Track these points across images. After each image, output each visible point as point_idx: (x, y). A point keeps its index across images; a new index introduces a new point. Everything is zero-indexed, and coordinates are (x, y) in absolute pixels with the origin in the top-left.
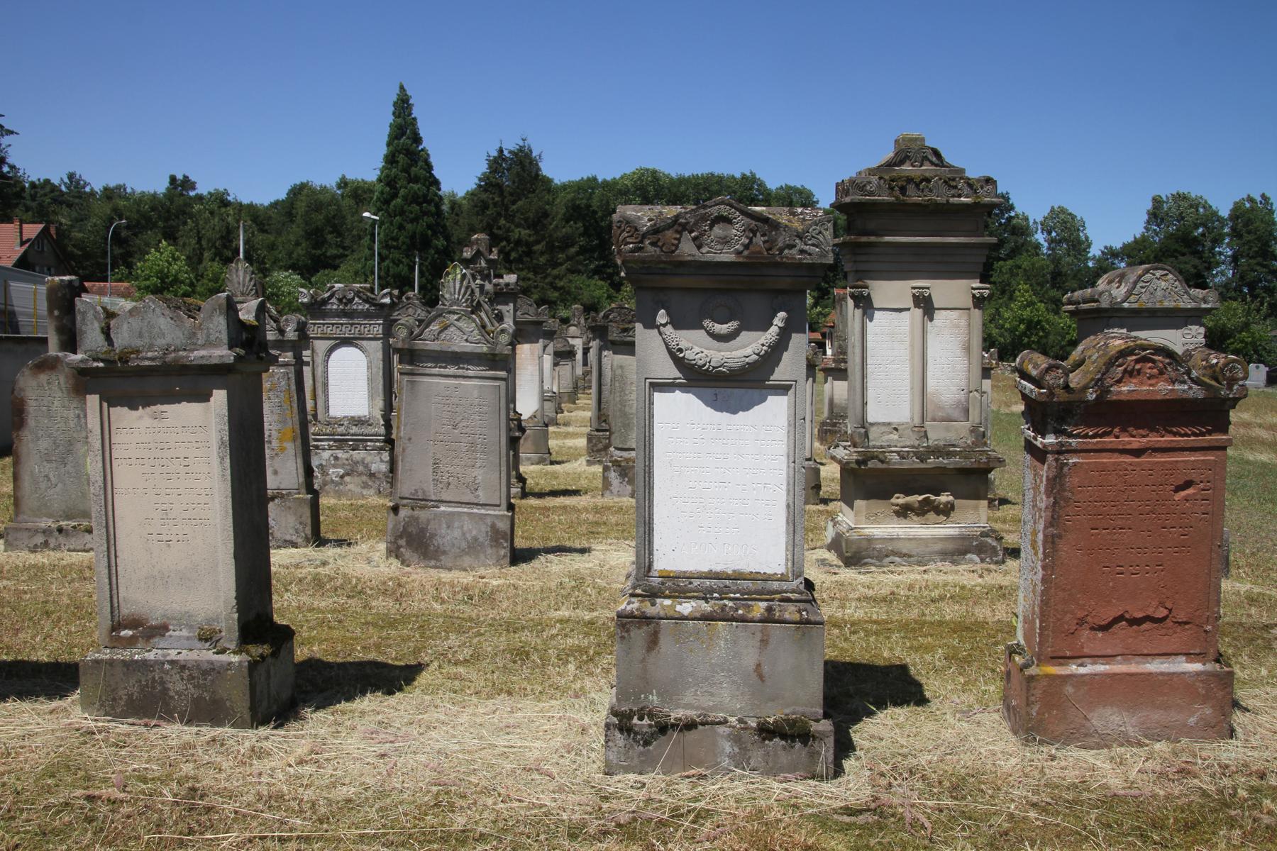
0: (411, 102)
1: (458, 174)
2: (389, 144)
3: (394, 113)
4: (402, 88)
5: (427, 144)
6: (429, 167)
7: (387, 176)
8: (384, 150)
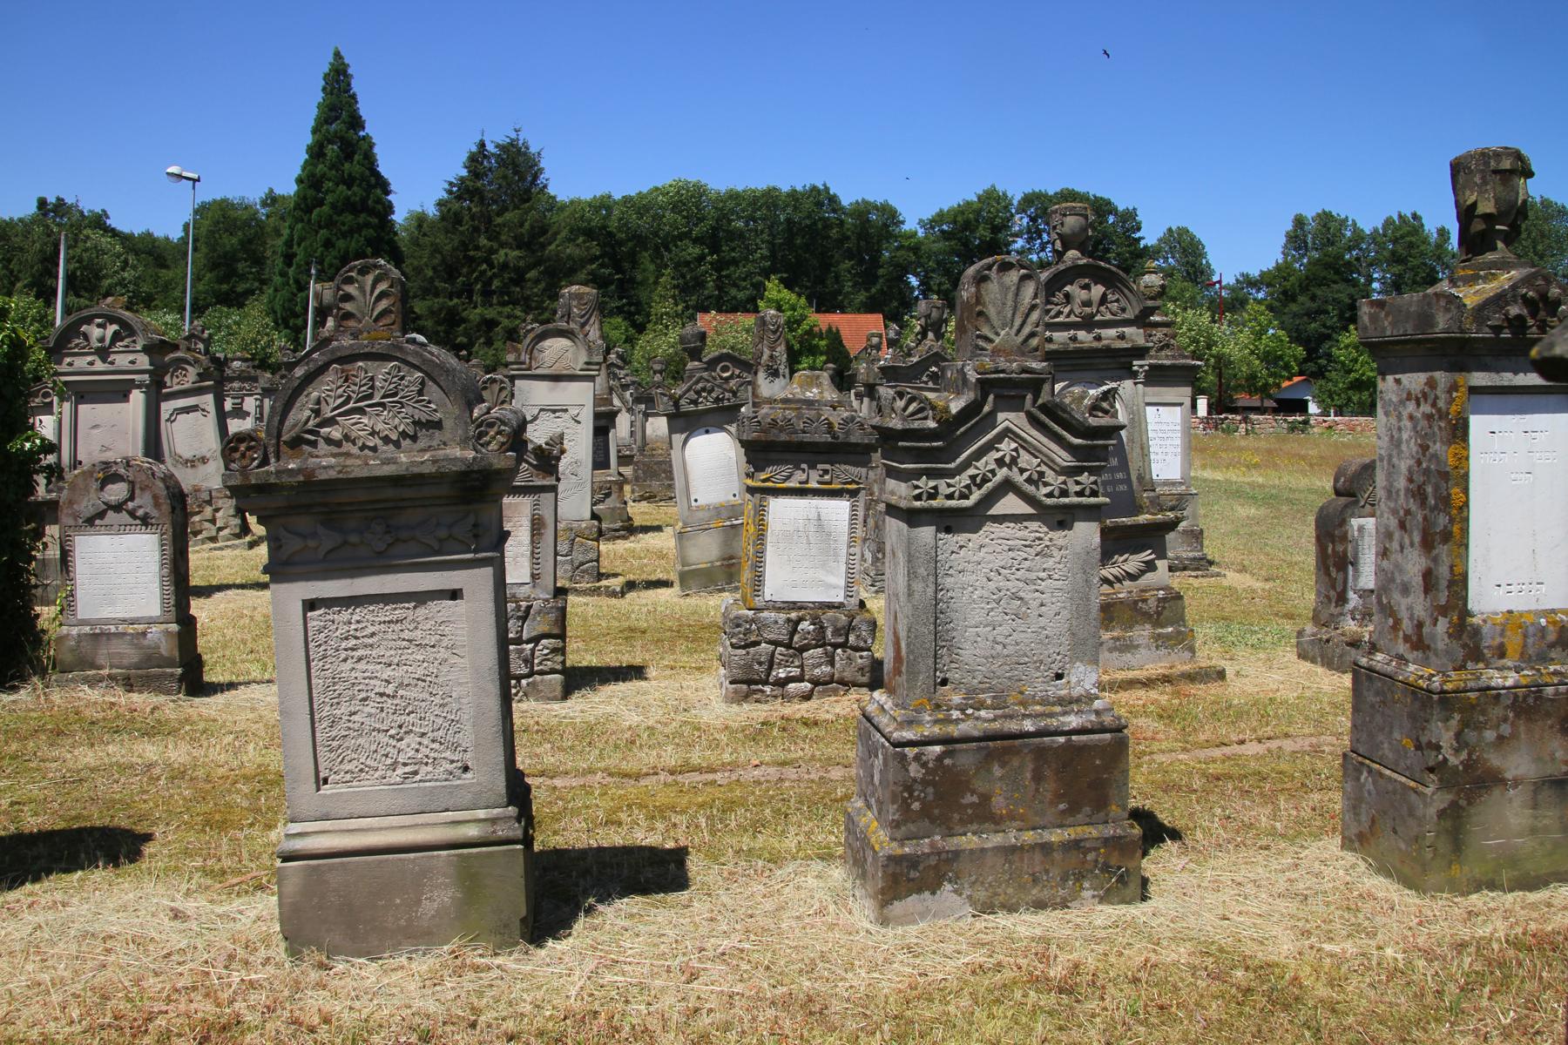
0: (350, 71)
1: (417, 185)
3: (324, 89)
5: (370, 129)
7: (312, 175)
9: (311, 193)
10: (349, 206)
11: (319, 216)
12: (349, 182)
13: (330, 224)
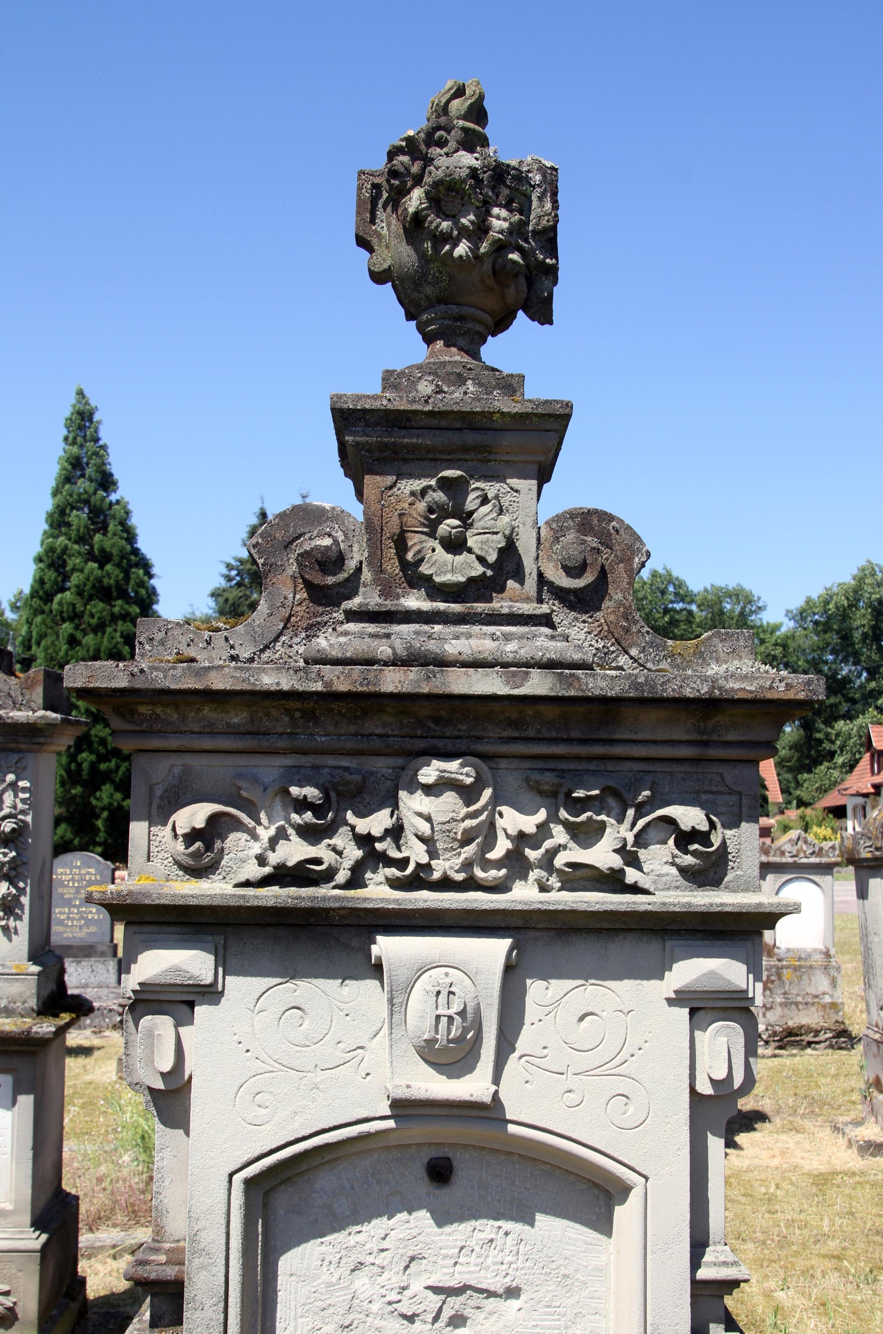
0: (96, 417)
2: (56, 492)
3: (66, 439)
4: (81, 393)
5: (127, 490)
6: (130, 535)
7: (51, 550)
8: (48, 504)
9: (51, 575)
10: (103, 592)
11: (60, 604)
12: (103, 559)
13: (75, 616)
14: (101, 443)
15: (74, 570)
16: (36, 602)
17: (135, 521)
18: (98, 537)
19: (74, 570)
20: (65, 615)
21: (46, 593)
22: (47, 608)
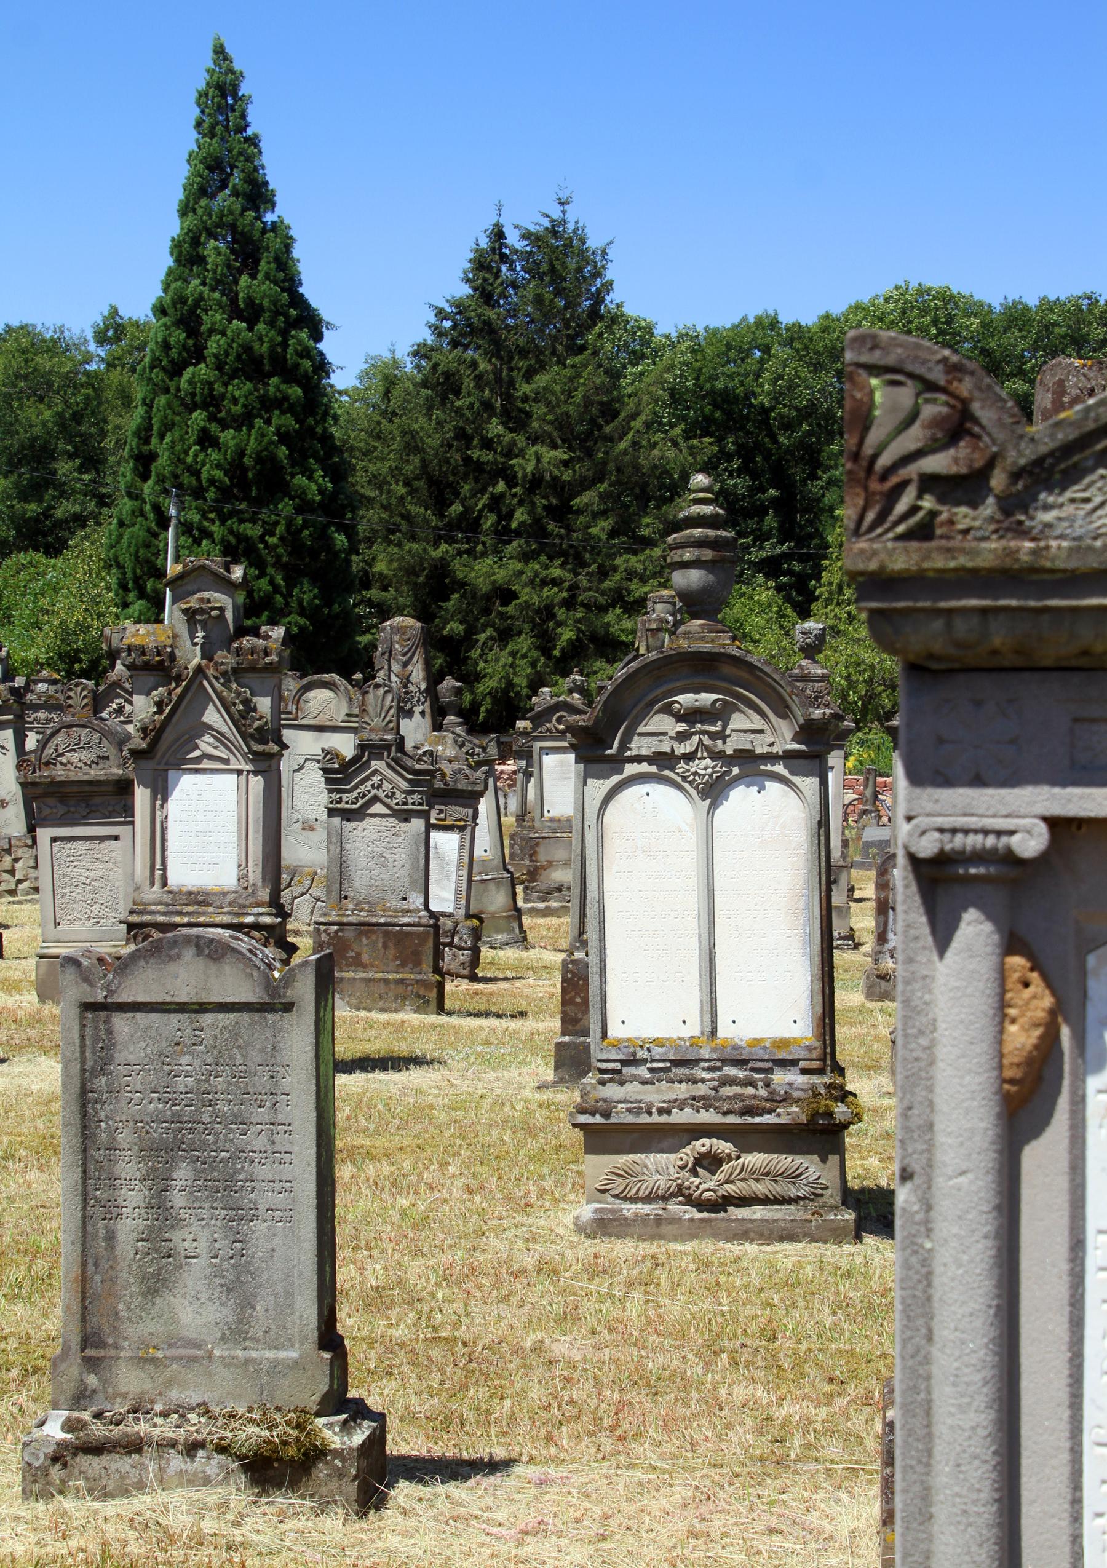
1: (376, 308)
6: (289, 282)
7: (180, 300)
10: (251, 366)
11: (190, 382)
12: (251, 313)
13: (211, 402)
14: (250, 132)
15: (211, 331)
16: (157, 375)
17: (297, 252)
18: (244, 280)
19: (211, 331)
20: (198, 399)
21: (172, 362)
22: (172, 385)
